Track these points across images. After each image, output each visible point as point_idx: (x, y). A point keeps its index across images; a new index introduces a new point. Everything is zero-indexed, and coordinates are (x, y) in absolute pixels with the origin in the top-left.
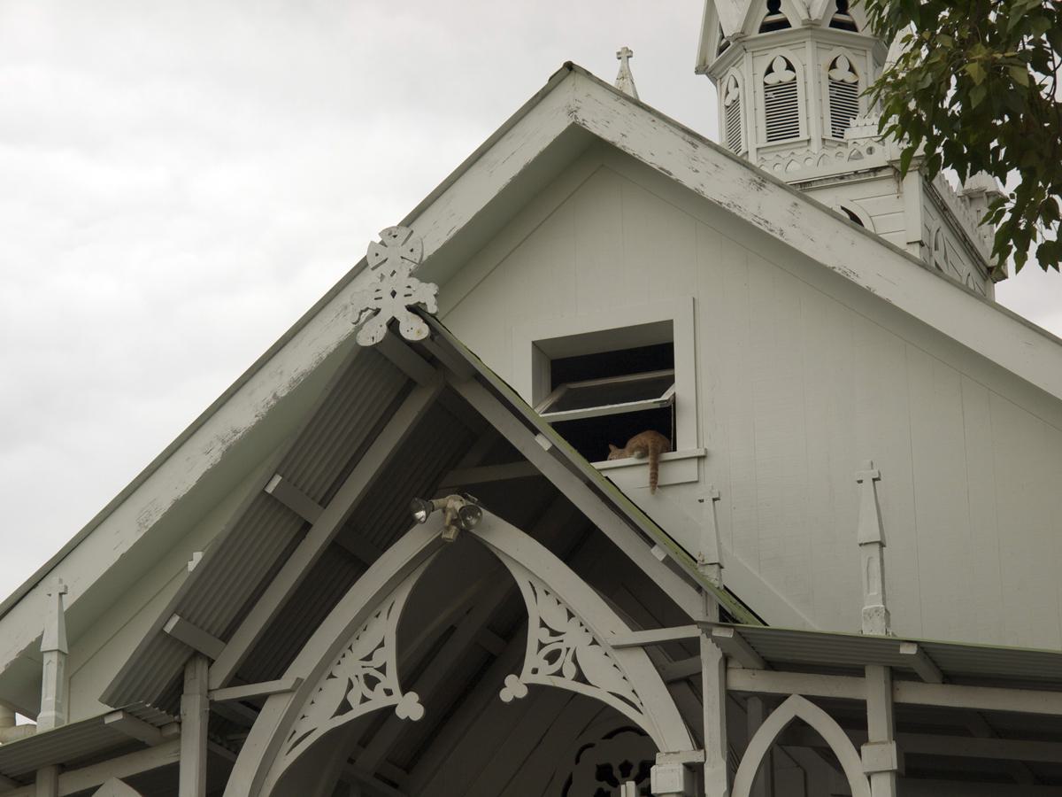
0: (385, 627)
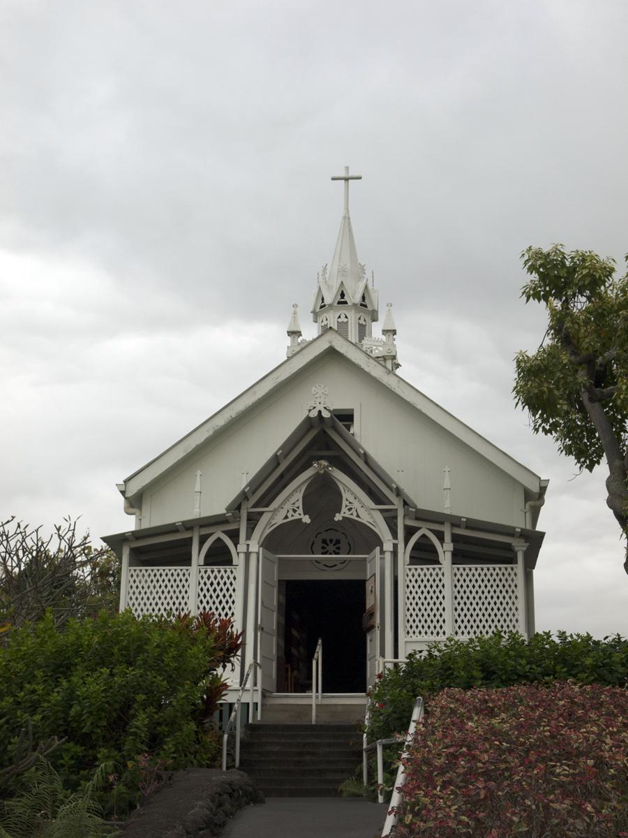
0: (299, 496)
